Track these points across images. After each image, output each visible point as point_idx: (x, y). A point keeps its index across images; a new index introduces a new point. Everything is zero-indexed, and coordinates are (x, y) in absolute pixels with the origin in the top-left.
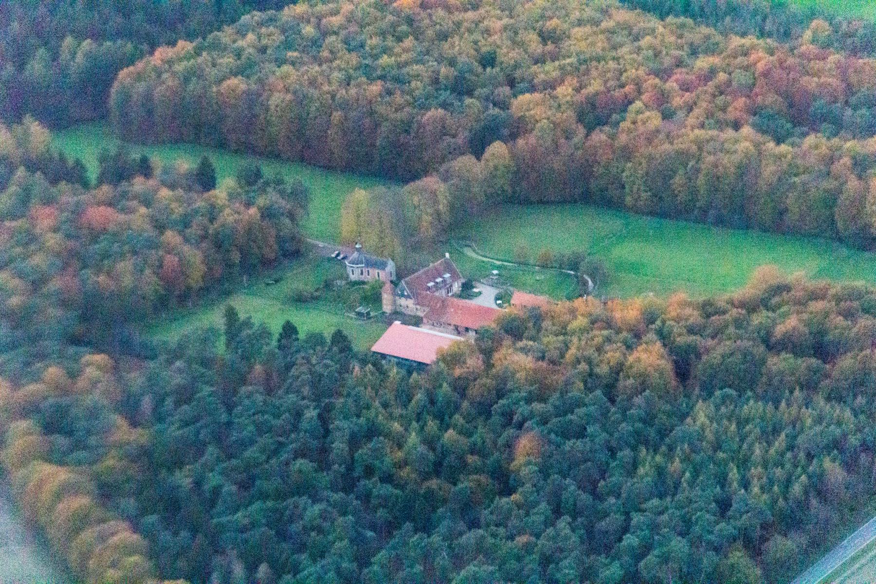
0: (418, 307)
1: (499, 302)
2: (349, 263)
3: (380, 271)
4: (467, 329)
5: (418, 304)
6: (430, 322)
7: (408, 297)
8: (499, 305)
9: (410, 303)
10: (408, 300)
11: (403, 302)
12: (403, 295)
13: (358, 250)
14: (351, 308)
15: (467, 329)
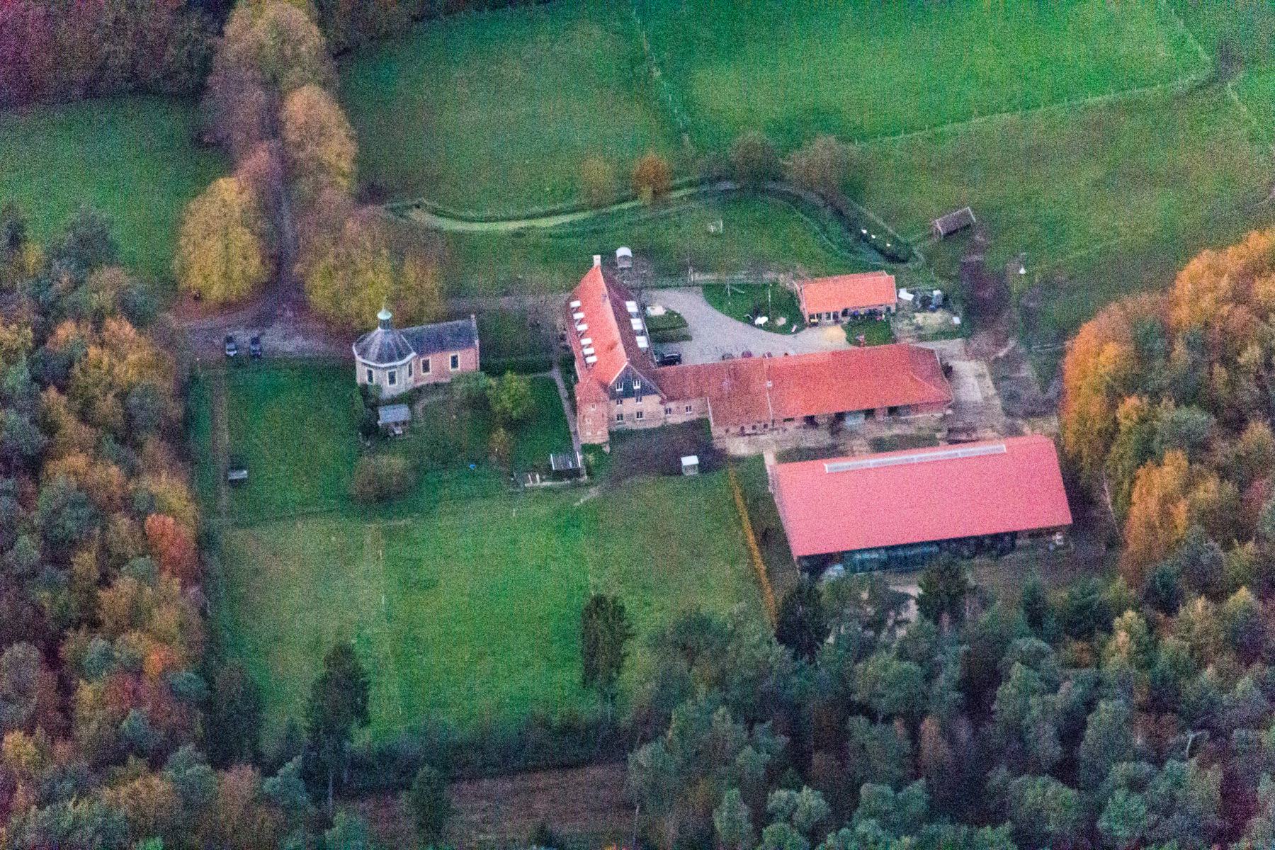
0: (672, 405)
1: (761, 320)
2: (380, 358)
3: (459, 354)
4: (840, 417)
5: (671, 399)
6: (733, 430)
7: (645, 391)
8: (768, 327)
9: (651, 404)
11: (630, 406)
12: (629, 393)
13: (385, 324)
14: (513, 468)
15: (840, 417)
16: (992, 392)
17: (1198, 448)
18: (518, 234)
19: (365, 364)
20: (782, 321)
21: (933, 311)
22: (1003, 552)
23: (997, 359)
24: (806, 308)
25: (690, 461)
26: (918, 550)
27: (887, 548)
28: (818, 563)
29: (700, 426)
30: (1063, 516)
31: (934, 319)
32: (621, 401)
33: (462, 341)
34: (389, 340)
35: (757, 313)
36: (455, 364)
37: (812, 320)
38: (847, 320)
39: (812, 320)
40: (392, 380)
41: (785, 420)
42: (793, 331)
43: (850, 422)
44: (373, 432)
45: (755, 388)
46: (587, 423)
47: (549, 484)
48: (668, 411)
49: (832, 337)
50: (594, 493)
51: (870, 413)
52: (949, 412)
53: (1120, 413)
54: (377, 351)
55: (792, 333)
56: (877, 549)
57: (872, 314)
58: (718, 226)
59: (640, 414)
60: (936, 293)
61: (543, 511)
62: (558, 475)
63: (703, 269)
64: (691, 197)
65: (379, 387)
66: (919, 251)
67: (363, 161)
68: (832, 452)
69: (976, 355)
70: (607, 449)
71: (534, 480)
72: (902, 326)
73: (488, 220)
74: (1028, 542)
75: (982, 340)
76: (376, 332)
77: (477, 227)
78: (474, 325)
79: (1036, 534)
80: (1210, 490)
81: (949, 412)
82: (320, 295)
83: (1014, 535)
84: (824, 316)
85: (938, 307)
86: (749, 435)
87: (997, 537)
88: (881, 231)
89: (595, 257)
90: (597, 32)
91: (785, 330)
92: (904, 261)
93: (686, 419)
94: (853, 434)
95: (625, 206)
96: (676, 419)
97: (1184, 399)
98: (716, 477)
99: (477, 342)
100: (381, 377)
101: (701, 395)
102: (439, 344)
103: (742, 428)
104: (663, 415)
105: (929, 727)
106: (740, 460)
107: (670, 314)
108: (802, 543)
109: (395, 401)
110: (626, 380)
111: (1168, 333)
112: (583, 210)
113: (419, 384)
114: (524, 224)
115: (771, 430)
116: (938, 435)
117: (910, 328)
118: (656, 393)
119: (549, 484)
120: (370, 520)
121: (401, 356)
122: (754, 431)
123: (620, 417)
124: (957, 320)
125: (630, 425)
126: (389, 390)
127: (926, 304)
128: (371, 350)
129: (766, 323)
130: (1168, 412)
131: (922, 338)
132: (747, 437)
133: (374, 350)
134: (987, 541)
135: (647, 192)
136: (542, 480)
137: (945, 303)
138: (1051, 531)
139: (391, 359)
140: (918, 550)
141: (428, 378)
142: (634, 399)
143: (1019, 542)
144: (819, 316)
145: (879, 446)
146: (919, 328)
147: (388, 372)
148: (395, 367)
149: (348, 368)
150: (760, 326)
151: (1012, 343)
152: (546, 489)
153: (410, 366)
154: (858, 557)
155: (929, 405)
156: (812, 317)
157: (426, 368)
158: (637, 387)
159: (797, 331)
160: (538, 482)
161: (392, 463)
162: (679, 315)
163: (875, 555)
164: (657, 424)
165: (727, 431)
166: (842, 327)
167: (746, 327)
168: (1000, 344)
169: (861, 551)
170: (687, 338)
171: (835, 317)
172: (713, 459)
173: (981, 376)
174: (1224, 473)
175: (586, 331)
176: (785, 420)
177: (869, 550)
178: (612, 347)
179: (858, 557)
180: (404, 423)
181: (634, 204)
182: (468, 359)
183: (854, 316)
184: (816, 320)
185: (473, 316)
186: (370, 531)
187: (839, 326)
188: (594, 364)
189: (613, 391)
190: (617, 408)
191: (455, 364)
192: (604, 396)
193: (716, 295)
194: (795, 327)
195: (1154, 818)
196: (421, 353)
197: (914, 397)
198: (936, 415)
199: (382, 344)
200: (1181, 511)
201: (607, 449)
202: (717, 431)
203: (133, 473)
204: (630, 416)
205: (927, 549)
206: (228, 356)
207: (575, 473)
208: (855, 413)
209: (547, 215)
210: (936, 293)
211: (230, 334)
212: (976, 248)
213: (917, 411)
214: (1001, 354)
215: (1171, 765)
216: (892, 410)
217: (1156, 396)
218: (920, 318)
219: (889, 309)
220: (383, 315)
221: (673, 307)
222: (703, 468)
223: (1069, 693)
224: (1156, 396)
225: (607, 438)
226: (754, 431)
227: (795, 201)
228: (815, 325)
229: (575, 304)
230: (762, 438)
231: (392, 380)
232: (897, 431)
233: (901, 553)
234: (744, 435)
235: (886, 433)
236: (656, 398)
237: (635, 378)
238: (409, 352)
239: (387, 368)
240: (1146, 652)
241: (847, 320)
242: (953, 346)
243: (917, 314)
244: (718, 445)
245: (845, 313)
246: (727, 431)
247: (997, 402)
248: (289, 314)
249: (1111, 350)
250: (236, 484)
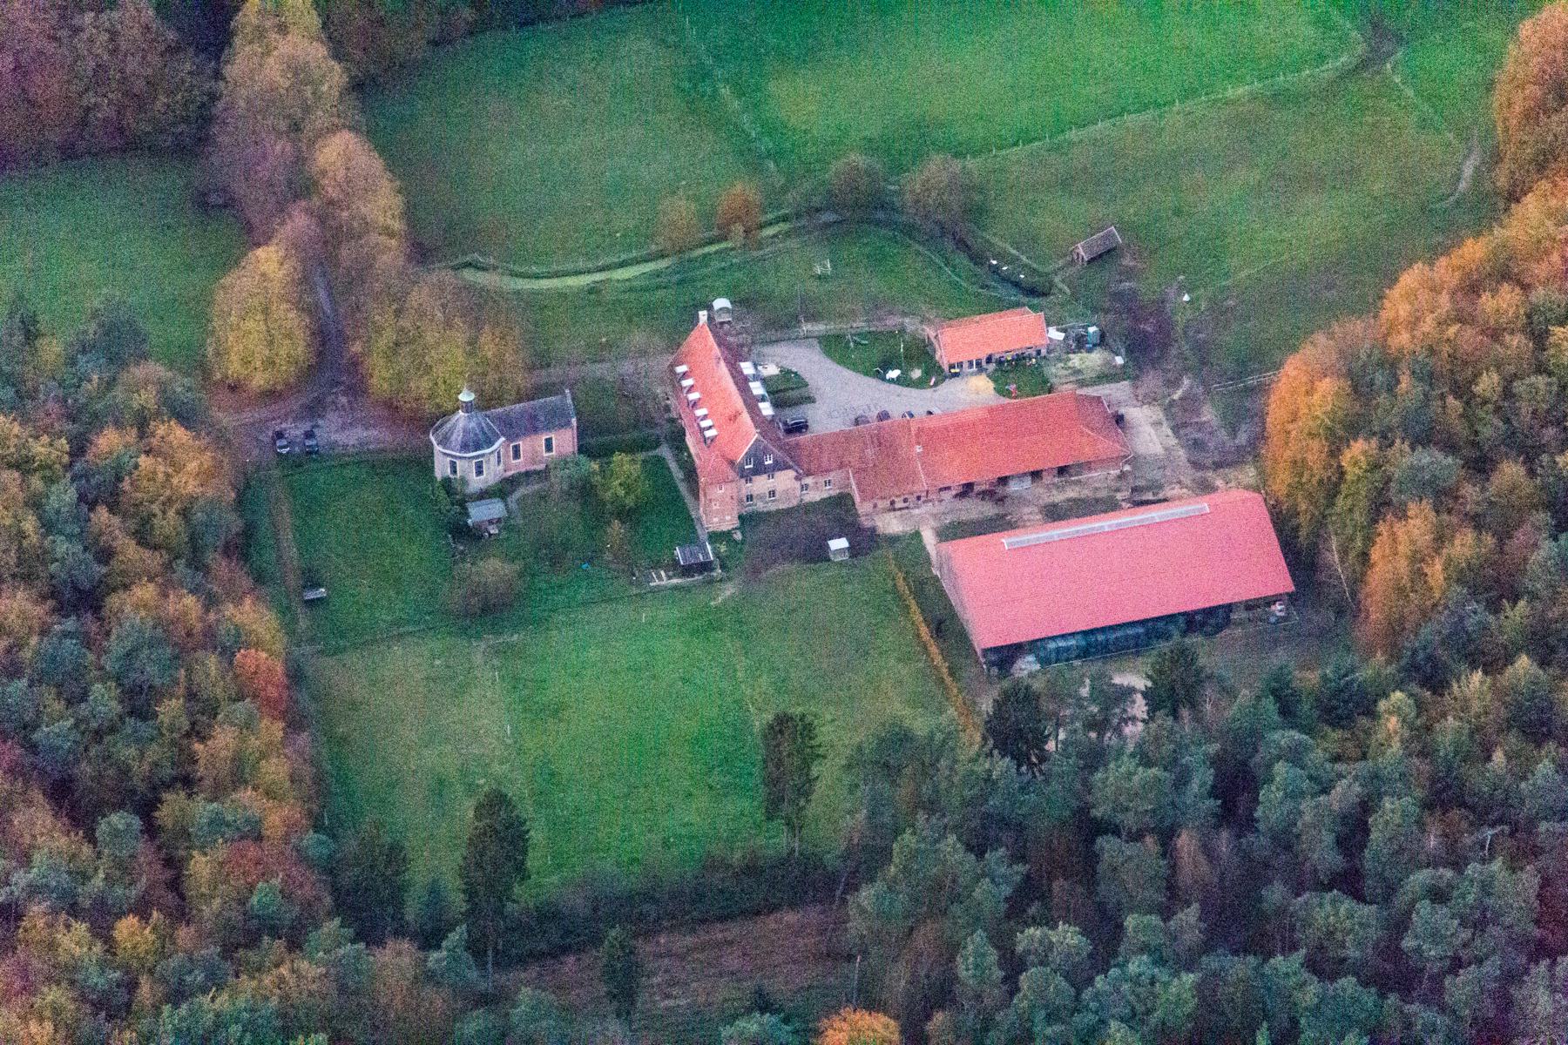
0: (809, 480)
1: (894, 374)
2: (465, 447)
3: (552, 435)
4: (1003, 481)
5: (808, 474)
7: (779, 466)
8: (902, 381)
9: (784, 481)
10: (778, 474)
11: (761, 484)
12: (760, 469)
13: (468, 407)
15: (1003, 481)
16: (1173, 441)
17: (1443, 496)
18: (593, 290)
19: (445, 454)
20: (917, 374)
21: (1090, 351)
22: (1219, 628)
23: (1172, 403)
24: (943, 357)
25: (839, 544)
26: (1119, 634)
27: (1085, 633)
28: (1006, 656)
29: (842, 502)
30: (1282, 582)
31: (1094, 360)
32: (751, 480)
33: (556, 419)
34: (472, 425)
35: (887, 365)
36: (549, 447)
37: (953, 371)
38: (992, 367)
39: (953, 371)
40: (479, 472)
41: (941, 490)
42: (932, 384)
43: (1013, 487)
44: (465, 533)
45: (902, 453)
46: (714, 508)
47: (675, 581)
48: (805, 487)
49: (977, 391)
50: (729, 590)
51: (1036, 475)
52: (1127, 468)
53: (1346, 459)
54: (459, 439)
55: (931, 387)
56: (1073, 634)
57: (1020, 359)
58: (824, 266)
59: (772, 493)
60: (1092, 330)
61: (674, 614)
62: (687, 571)
63: (813, 317)
64: (788, 234)
65: (464, 481)
66: (1063, 281)
67: (410, 214)
68: (1000, 524)
69: (1150, 400)
70: (738, 536)
71: (660, 578)
72: (1054, 371)
73: (557, 275)
74: (1244, 615)
75: (1152, 381)
76: (456, 417)
77: (545, 284)
78: (569, 401)
79: (1250, 606)
80: (1464, 545)
81: (1127, 468)
82: (380, 377)
83: (1229, 608)
84: (966, 365)
85: (1095, 345)
86: (900, 509)
87: (1210, 612)
88: (1013, 260)
89: (701, 313)
90: (646, 44)
91: (920, 384)
92: (1045, 295)
93: (825, 495)
94: (1021, 500)
95: (713, 248)
96: (814, 496)
97: (1422, 439)
98: (866, 561)
99: (574, 421)
100: (466, 468)
101: (841, 466)
102: (532, 425)
103: (893, 503)
104: (798, 492)
105: (1186, 842)
106: (893, 540)
107: (786, 373)
108: (985, 633)
109: (483, 495)
110: (756, 455)
111: (1390, 364)
112: (663, 257)
113: (509, 473)
114: (598, 277)
115: (924, 502)
116: (1119, 496)
117: (1066, 372)
118: (790, 467)
119: (675, 581)
120: (479, 637)
121: (490, 443)
122: (906, 505)
123: (750, 498)
124: (1119, 360)
125: (760, 506)
126: (476, 483)
127: (1081, 343)
128: (453, 438)
129: (898, 377)
130: (1406, 458)
131: (1082, 384)
132: (898, 513)
133: (457, 437)
134: (1198, 618)
135: (738, 229)
136: (669, 578)
137: (1102, 341)
138: (1269, 602)
139: (477, 447)
140: (1119, 634)
141: (519, 466)
142: (765, 476)
143: (1234, 616)
144: (960, 365)
145: (1054, 514)
146: (1078, 372)
147: (474, 461)
148: (483, 455)
149: (424, 463)
150: (892, 381)
151: (1186, 382)
152: (675, 588)
153: (499, 453)
154: (1052, 645)
155: (1104, 462)
156: (952, 366)
157: (517, 455)
158: (769, 462)
159: (936, 384)
160: (662, 580)
161: (493, 569)
162: (796, 373)
163: (1072, 642)
164: (795, 502)
165: (875, 506)
166: (988, 376)
167: (873, 382)
168: (1174, 383)
169: (1053, 638)
170: (810, 400)
171: (979, 364)
172: (865, 541)
173: (1157, 424)
174: (1477, 522)
175: (699, 399)
176: (941, 490)
177: (1063, 636)
178: (734, 417)
179: (1052, 645)
180: (499, 520)
181: (723, 245)
182: (565, 441)
183: (1000, 362)
184: (957, 370)
185: (567, 391)
186: (478, 651)
187: (984, 376)
188: (713, 439)
189: (743, 470)
190: (747, 488)
191: (549, 447)
192: (732, 474)
193: (834, 346)
194: (933, 380)
195: (1465, 935)
196: (510, 439)
197: (1088, 453)
198: (1112, 472)
199: (466, 431)
200: (1436, 571)
201: (738, 536)
202: (863, 508)
203: (211, 602)
204: (761, 497)
205: (1130, 632)
206: (280, 454)
207: (705, 567)
208: (1022, 476)
209: (623, 265)
210: (1092, 330)
211: (278, 429)
212: (1129, 274)
213: (1090, 469)
214: (1176, 397)
215: (1472, 869)
216: (1062, 471)
217: (1386, 440)
218: (1076, 360)
219: (1039, 352)
220: (466, 397)
221: (787, 364)
222: (854, 550)
223: (1345, 793)
224: (1386, 440)
225: (737, 523)
226: (906, 505)
227: (910, 231)
228: (956, 375)
229: (681, 369)
230: (917, 511)
231: (479, 472)
232: (1071, 493)
233: (1101, 637)
234: (894, 510)
235: (1058, 497)
236: (791, 473)
237: (765, 451)
238: (498, 438)
239: (474, 457)
240: (1421, 737)
241: (992, 367)
242: (1117, 392)
243: (1071, 356)
244: (867, 524)
245: (989, 360)
246: (875, 506)
247: (1182, 453)
248: (343, 400)
249: (1327, 386)
250: (311, 603)
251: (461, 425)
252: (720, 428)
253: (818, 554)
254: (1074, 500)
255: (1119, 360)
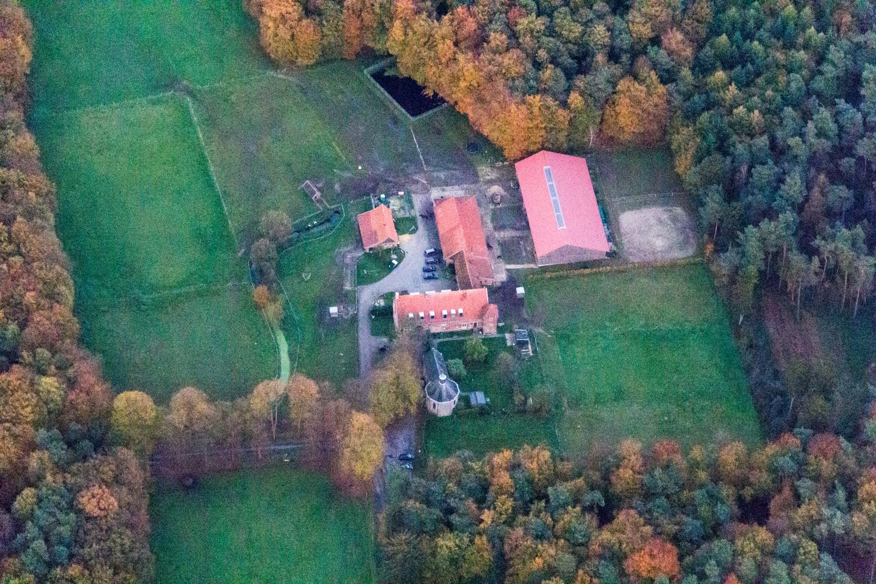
1: (395, 262)
25: (520, 290)
31: (395, 203)
72: (401, 214)
76: (444, 387)
133: (451, 391)
136: (528, 348)
151: (416, 177)
167: (394, 272)
173: (444, 190)
202: (490, 282)
243: (391, 207)
244: (499, 284)
251: (449, 388)
252: (460, 306)
253: (519, 302)
254: (492, 222)
255: (401, 193)
